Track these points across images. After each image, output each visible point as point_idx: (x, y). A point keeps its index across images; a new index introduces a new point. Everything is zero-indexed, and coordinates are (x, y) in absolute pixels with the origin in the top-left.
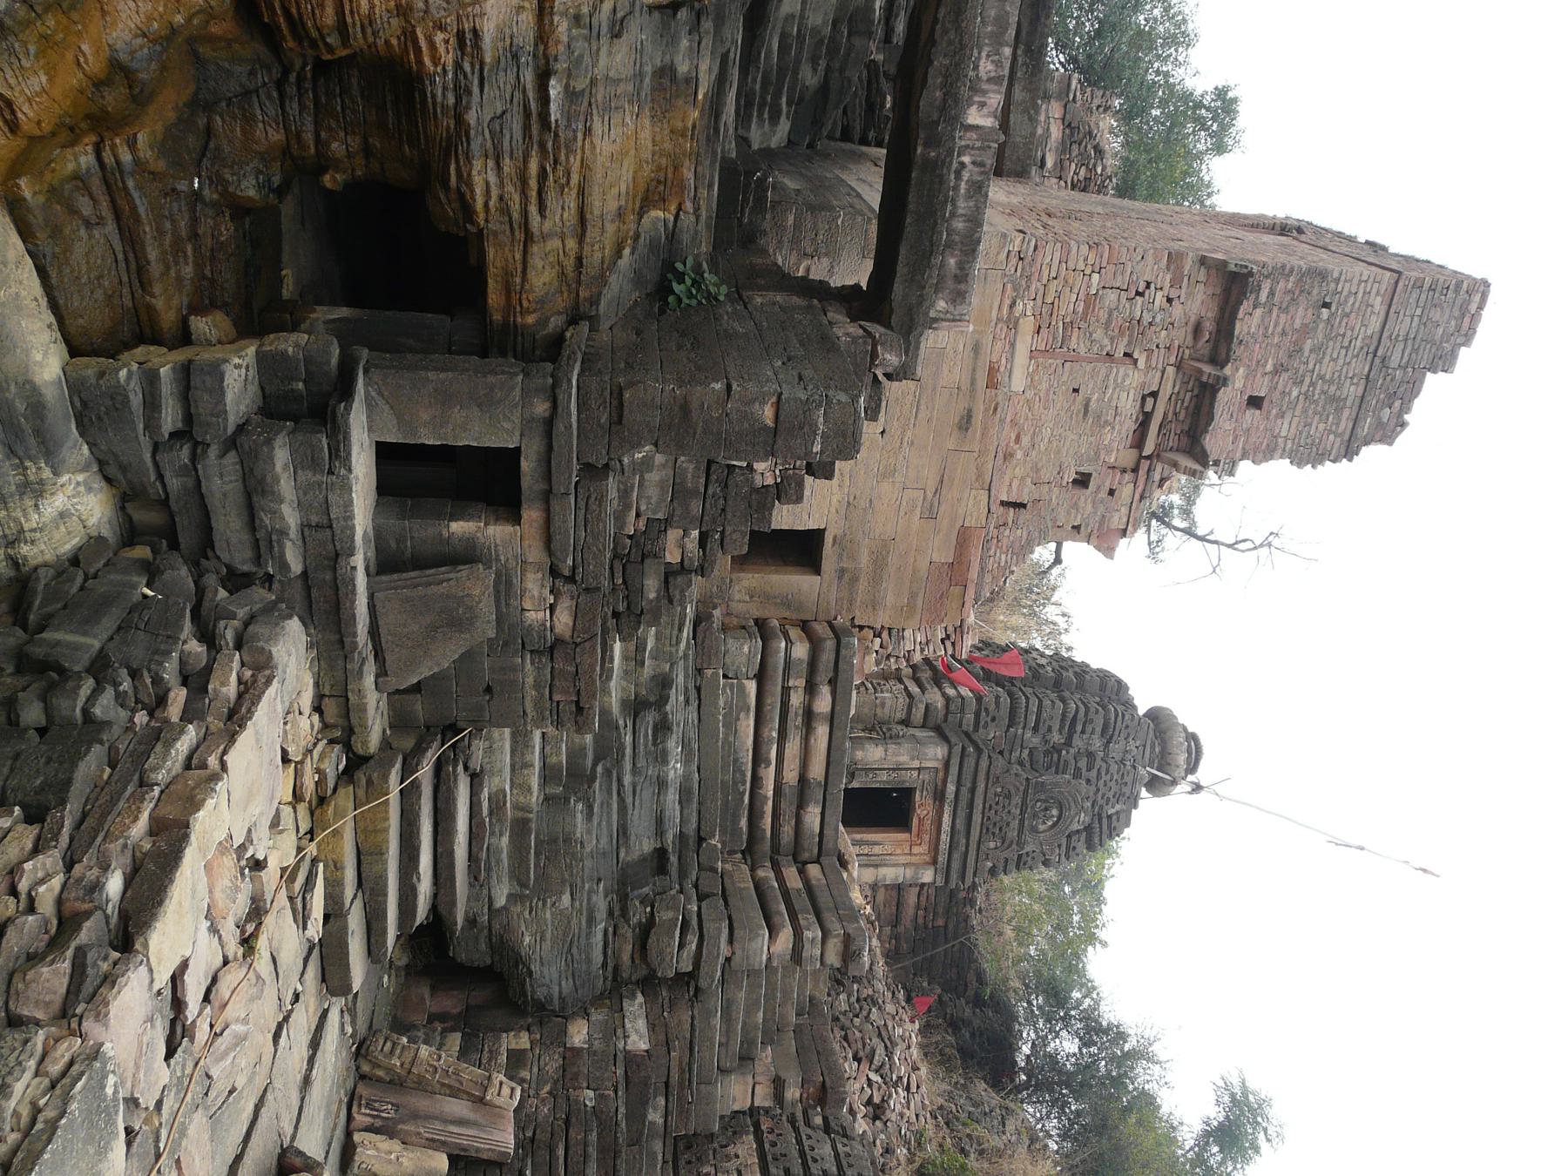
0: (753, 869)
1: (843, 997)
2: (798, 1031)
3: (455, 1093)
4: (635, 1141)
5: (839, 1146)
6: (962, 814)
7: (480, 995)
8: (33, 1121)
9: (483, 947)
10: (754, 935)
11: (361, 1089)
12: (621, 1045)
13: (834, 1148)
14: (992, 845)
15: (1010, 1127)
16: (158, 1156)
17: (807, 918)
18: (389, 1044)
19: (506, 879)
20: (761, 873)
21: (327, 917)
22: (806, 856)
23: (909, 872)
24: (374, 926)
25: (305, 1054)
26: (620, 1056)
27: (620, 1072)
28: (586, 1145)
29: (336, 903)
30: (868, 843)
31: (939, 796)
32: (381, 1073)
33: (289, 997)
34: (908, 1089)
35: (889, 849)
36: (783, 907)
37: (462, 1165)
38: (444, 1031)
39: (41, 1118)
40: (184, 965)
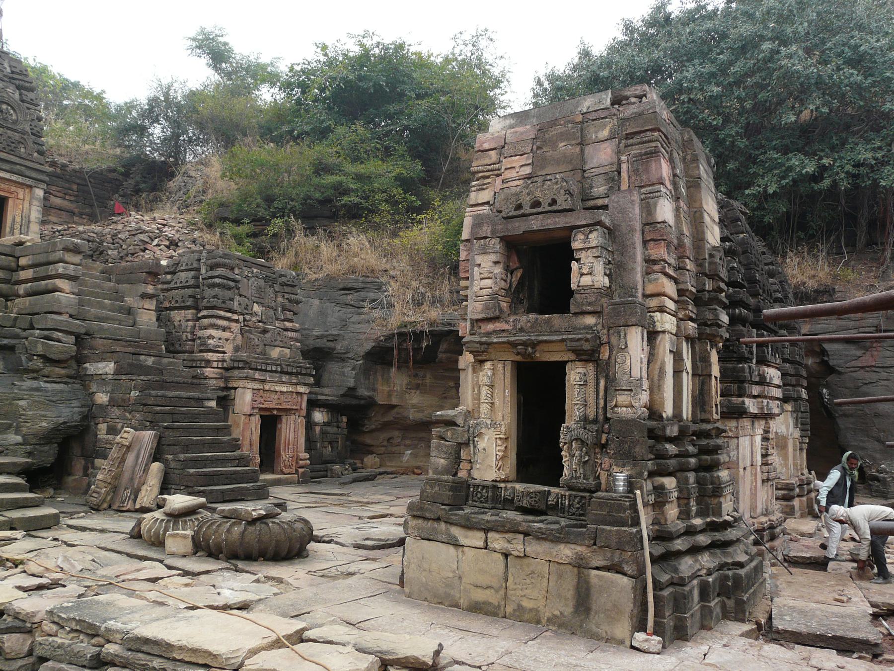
0: (19, 296)
1: (110, 252)
2: (118, 282)
3: (123, 460)
4: (161, 372)
5: (182, 268)
7: (76, 450)
8: (77, 631)
9: (46, 448)
10: (58, 301)
11: (115, 507)
12: (110, 377)
13: (183, 271)
14: (23, 150)
15: (193, 174)
16: (111, 584)
17: (51, 270)
18: (94, 495)
19: (5, 436)
20: (21, 292)
21: (12, 529)
22: (13, 265)
23: (35, 203)
24: (21, 505)
25: (87, 533)
26: (116, 377)
27: (124, 377)
28: (157, 396)
29: (4, 525)
32: (109, 498)
33: (55, 543)
34: (164, 225)
35: (18, 212)
36: (43, 282)
37: (158, 456)
38: (93, 468)
39: (75, 628)
40: (19, 588)
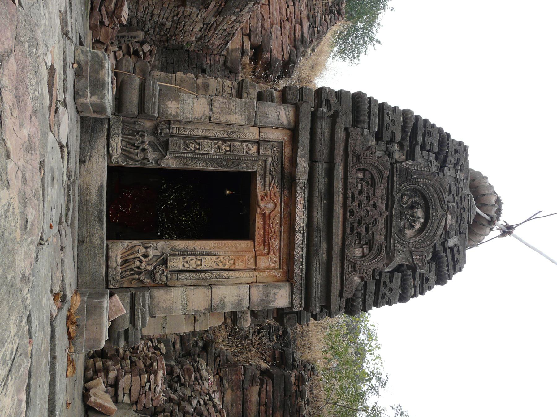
6: (320, 203)
14: (358, 252)
30: (195, 254)
31: (288, 182)
35: (225, 260)
